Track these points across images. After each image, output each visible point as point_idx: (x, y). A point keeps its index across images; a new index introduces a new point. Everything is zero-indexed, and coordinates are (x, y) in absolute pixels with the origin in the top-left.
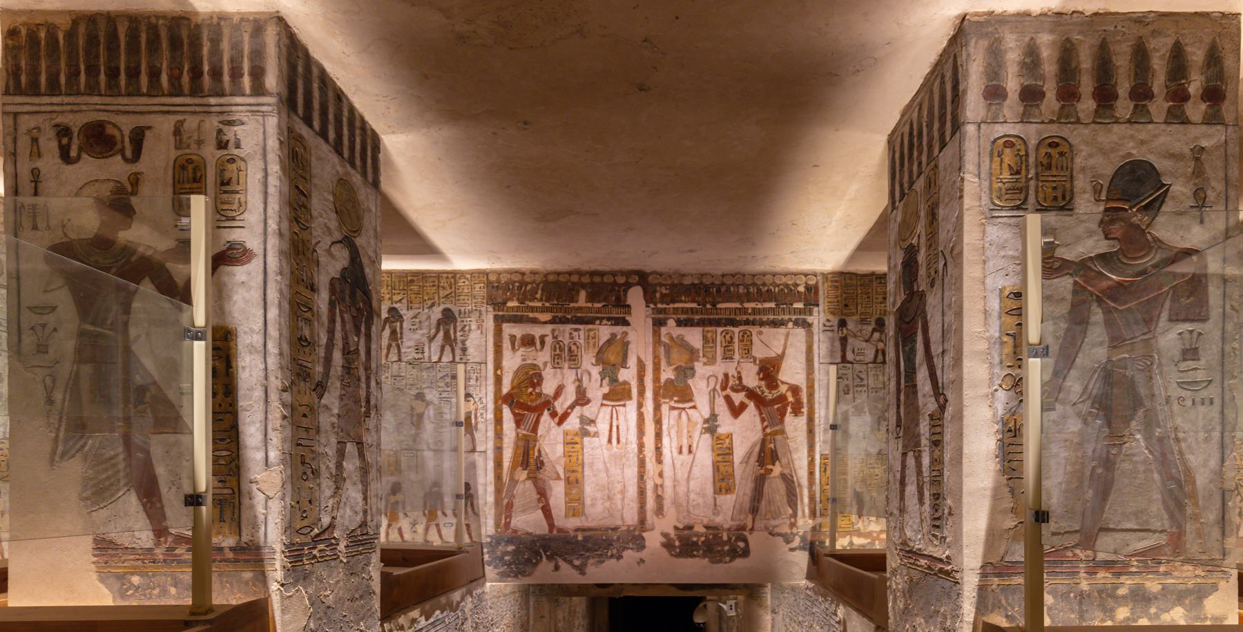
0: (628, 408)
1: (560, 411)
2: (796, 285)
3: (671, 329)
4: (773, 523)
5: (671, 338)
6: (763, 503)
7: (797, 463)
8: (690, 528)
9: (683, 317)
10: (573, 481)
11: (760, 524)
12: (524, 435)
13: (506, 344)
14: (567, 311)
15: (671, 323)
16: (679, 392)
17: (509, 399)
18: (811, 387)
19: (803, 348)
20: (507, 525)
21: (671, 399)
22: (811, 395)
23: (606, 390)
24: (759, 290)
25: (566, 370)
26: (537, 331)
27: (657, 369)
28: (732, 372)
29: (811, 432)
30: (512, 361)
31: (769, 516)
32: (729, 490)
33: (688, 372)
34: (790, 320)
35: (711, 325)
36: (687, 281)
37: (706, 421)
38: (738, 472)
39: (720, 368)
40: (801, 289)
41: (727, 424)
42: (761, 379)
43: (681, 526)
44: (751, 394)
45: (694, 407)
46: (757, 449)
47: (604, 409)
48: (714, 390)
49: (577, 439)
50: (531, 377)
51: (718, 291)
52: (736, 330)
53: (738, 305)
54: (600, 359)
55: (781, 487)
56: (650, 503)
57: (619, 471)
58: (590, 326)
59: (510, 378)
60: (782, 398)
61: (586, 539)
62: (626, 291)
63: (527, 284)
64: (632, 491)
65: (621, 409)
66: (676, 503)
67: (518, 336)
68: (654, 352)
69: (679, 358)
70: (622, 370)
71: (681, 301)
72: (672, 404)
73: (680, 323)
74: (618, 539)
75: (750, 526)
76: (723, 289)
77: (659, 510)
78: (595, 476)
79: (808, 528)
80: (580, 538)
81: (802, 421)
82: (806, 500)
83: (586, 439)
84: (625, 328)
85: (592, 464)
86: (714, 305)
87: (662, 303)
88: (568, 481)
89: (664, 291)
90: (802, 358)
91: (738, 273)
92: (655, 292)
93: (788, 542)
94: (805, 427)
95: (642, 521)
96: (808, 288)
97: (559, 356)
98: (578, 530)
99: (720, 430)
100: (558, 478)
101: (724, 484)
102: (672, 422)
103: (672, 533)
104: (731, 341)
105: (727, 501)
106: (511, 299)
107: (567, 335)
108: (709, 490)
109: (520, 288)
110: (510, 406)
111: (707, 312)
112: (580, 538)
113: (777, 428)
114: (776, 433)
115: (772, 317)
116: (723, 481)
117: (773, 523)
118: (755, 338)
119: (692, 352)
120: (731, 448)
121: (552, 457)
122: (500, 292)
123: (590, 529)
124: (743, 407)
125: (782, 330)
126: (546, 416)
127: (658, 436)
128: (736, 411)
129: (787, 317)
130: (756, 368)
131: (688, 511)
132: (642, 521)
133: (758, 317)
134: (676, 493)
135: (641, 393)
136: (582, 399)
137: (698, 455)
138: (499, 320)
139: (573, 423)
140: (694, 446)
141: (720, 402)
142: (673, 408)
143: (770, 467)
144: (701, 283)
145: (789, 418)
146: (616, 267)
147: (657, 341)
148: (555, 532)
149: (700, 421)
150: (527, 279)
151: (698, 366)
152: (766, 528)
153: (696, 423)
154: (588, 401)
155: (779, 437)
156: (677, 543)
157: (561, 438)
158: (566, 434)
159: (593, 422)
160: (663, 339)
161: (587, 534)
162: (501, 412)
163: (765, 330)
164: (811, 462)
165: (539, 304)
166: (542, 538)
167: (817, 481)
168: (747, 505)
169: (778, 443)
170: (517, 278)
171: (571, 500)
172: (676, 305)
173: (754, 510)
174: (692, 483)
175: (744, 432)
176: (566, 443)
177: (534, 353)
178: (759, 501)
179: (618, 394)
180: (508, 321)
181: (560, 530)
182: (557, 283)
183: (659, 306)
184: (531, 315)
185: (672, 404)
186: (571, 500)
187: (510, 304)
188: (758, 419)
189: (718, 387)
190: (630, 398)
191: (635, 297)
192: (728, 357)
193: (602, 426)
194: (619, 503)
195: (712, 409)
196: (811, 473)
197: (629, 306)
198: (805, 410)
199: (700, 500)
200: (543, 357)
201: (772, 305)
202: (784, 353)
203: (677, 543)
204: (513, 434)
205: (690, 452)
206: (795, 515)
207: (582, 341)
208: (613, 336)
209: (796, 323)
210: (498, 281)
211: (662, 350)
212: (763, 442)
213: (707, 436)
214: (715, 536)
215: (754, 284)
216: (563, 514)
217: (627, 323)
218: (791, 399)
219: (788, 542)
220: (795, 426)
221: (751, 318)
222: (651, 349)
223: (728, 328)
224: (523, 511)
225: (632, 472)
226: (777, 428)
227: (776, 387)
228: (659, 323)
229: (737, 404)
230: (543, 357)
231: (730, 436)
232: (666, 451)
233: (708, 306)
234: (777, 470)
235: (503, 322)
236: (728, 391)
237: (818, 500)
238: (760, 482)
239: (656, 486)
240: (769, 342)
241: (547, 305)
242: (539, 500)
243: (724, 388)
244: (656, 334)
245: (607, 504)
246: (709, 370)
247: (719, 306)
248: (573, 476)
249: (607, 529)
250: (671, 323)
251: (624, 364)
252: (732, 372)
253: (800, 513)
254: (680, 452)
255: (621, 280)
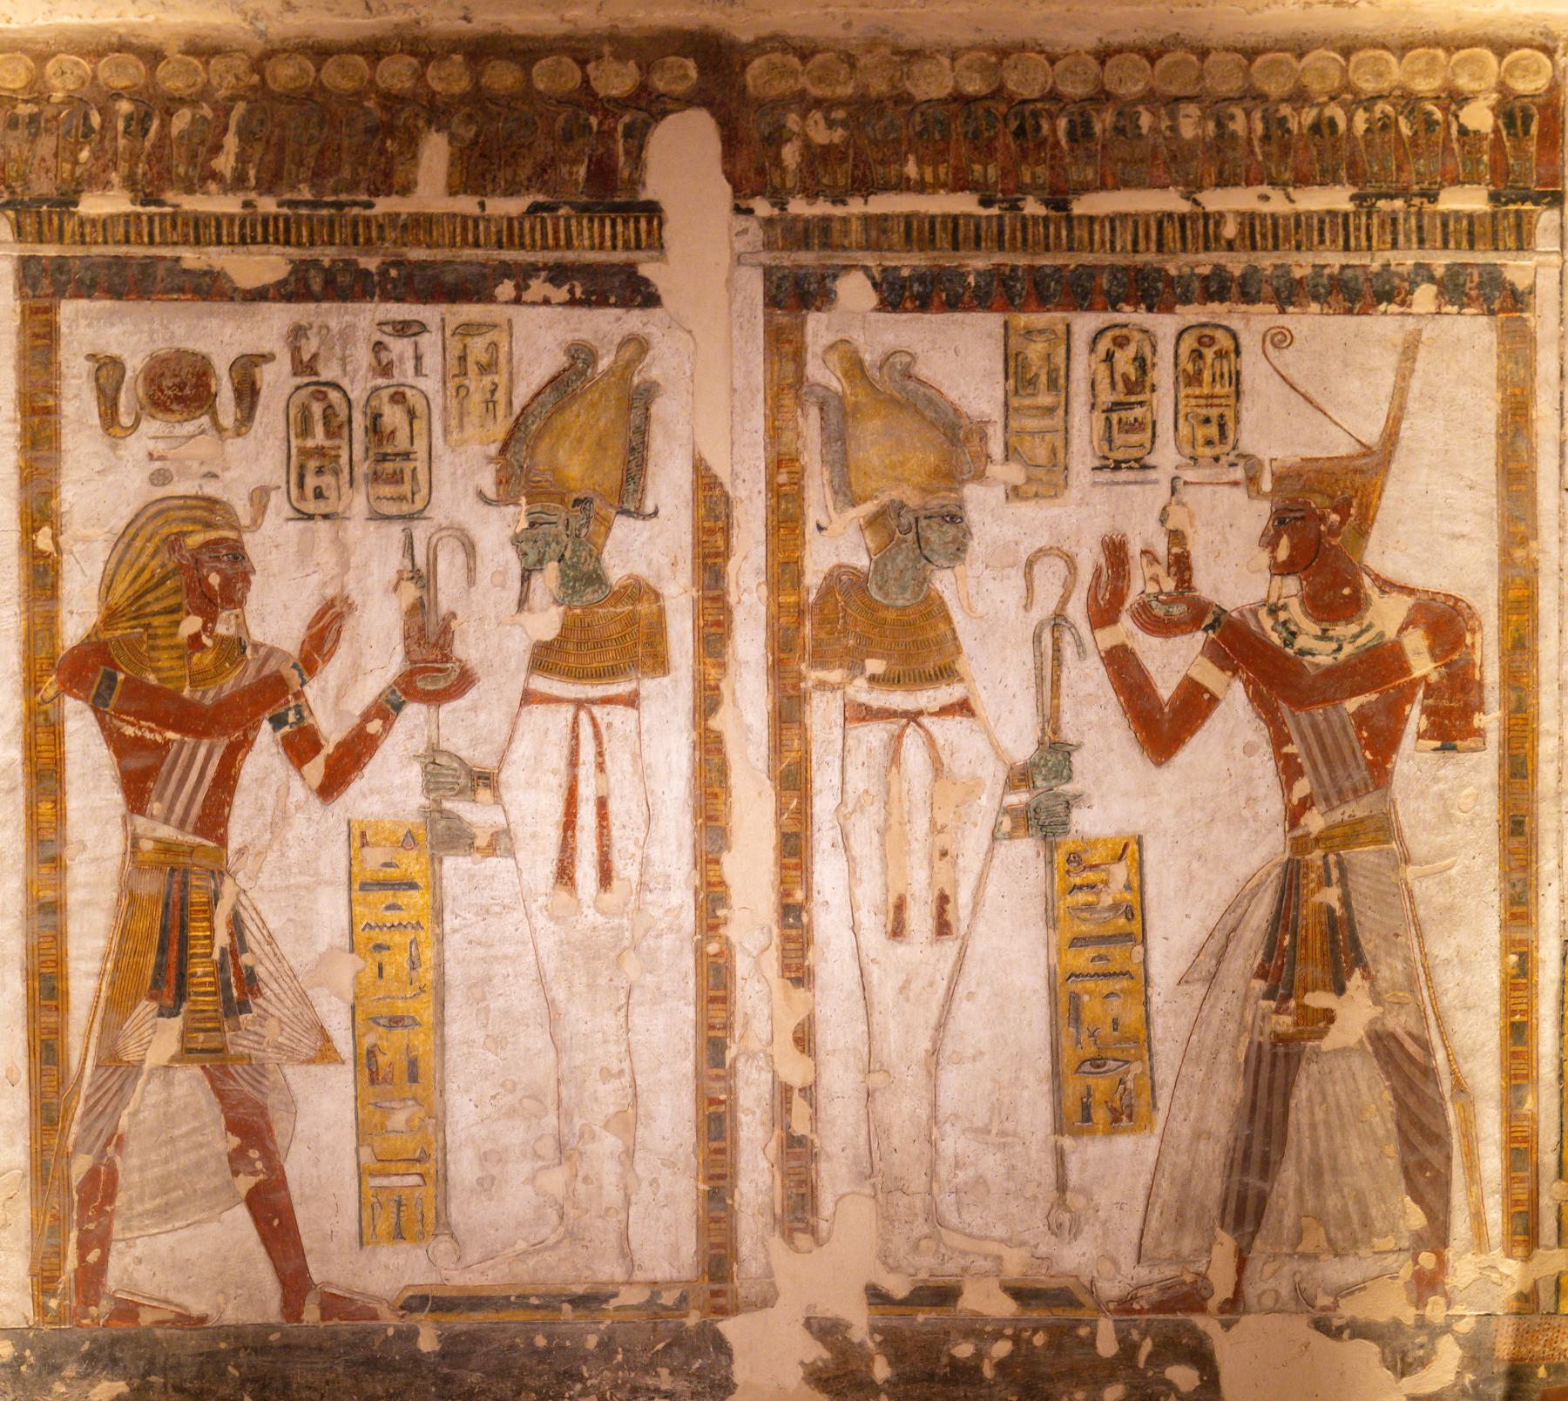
0: (651, 711)
1: (332, 729)
2: (1456, 99)
3: (852, 318)
4: (1336, 1272)
5: (855, 367)
6: (1288, 1175)
7: (1448, 980)
8: (943, 1295)
9: (910, 262)
10: (396, 1072)
11: (1270, 1278)
12: (166, 847)
13: (77, 401)
14: (362, 234)
15: (855, 291)
16: (890, 633)
17: (94, 671)
18: (1520, 605)
19: (1488, 410)
20: (91, 1278)
21: (854, 665)
22: (1520, 646)
23: (546, 623)
24: (1276, 127)
25: (357, 529)
26: (220, 337)
27: (786, 522)
28: (1144, 533)
29: (1517, 828)
30: (105, 487)
31: (1314, 1239)
32: (1124, 1115)
33: (935, 535)
34: (1423, 272)
35: (1042, 299)
36: (932, 84)
37: (1020, 777)
38: (1169, 1030)
39: (1085, 513)
40: (1479, 117)
41: (1117, 790)
42: (1281, 570)
43: (898, 1287)
44: (1236, 644)
45: (963, 708)
46: (1261, 912)
47: (537, 715)
48: (1058, 621)
49: (412, 864)
50: (192, 566)
51: (1080, 132)
52: (1165, 325)
53: (1171, 201)
54: (517, 471)
55: (1373, 1095)
56: (757, 1177)
57: (610, 1022)
58: (470, 312)
59: (96, 570)
60: (1381, 664)
61: (455, 1349)
62: (637, 137)
63: (171, 104)
64: (672, 1118)
65: (618, 716)
66: (873, 1173)
67: (135, 364)
68: (774, 433)
69: (892, 459)
70: (622, 528)
71: (902, 185)
72: (861, 692)
73: (895, 295)
74: (607, 1346)
75: (1222, 1287)
76: (1103, 122)
77: (799, 1210)
78: (497, 1042)
79: (1500, 1300)
80: (427, 1342)
81: (1475, 774)
82: (1492, 1163)
83: (454, 866)
84: (633, 320)
85: (480, 987)
86: (1058, 201)
87: (812, 196)
88: (370, 1067)
89: (821, 135)
90: (1482, 460)
91: (1177, 42)
92: (776, 139)
93: (1403, 1365)
94: (1489, 808)
95: (718, 1261)
96: (1512, 114)
97: (325, 459)
98: (416, 1303)
99: (1088, 822)
100: (325, 1053)
101: (1101, 1085)
102: (859, 780)
103: (860, 1322)
104: (1139, 383)
105: (1119, 1165)
106: (95, 181)
107: (362, 356)
108: (1034, 1110)
109: (138, 124)
110: (98, 706)
111: (1025, 235)
112: (427, 1342)
113: (1357, 809)
114: (1351, 834)
115: (1334, 259)
116: (1097, 1075)
117: (1336, 1272)
118: (1253, 367)
119: (955, 435)
120: (1134, 911)
121: (297, 955)
122: (46, 145)
123: (474, 1302)
124: (1194, 705)
125: (1385, 325)
126: (265, 754)
127: (794, 848)
128: (1163, 726)
129: (1406, 259)
130: (1256, 515)
131: (934, 1217)
132: (718, 1261)
133: (1266, 261)
134: (875, 1129)
135: (714, 635)
136: (433, 671)
137: (978, 947)
138: (43, 287)
139: (391, 786)
140: (964, 897)
141: (1087, 679)
142: (866, 714)
143: (1319, 999)
144: (998, 92)
145: (1413, 759)
146: (585, 17)
147: (787, 382)
148: (311, 1314)
149: (992, 775)
150: (172, 80)
151: (983, 504)
152: (1302, 1298)
153: (973, 788)
154: (465, 681)
155: (1363, 856)
156: (881, 1370)
157: (334, 860)
158: (359, 838)
159: (484, 780)
160: (816, 371)
161: (462, 1322)
162: (56, 732)
163: (1306, 322)
164: (1519, 979)
165: (229, 205)
166: (251, 1341)
167: (1547, 1071)
168: (1211, 1187)
169: (1361, 885)
170: (123, 74)
171: (386, 1163)
172: (881, 204)
173: (1245, 1212)
174: (952, 1081)
175: (1201, 827)
176: (362, 885)
177: (204, 446)
178: (1267, 1169)
179: (602, 643)
180: (86, 289)
181: (333, 1305)
182: (310, 99)
183: (798, 207)
184: (191, 258)
185: (861, 692)
186: (386, 1163)
187: (93, 205)
188: (1265, 767)
189: (1077, 611)
190: (658, 663)
191: (683, 162)
192: (1123, 461)
193: (531, 802)
194: (609, 1173)
195: (1050, 719)
196: (1518, 1032)
197: (652, 210)
198: (1490, 720)
199: (991, 1164)
200: (246, 464)
201: (1338, 198)
202: (1391, 437)
203: (881, 1370)
204: (115, 844)
205: (943, 927)
206: (1437, 1235)
207: (431, 384)
208: (581, 356)
209: (1453, 289)
210: (37, 91)
211: (810, 426)
212: (1292, 880)
213: (1026, 848)
214: (1061, 1335)
215: (1252, 96)
216: (348, 1224)
217: (643, 295)
218: (1423, 665)
219: (1403, 1365)
220: (1440, 796)
221: (1236, 264)
222: (757, 420)
223: (1131, 316)
224: (165, 1213)
225: (668, 1026)
226: (1357, 809)
227: (1354, 606)
228: (795, 295)
229: (1166, 690)
230: (246, 464)
231: (1130, 849)
232: (828, 924)
233: (1032, 207)
234: (1354, 1014)
235: (60, 293)
236: (1126, 630)
237: (1548, 1159)
238: (1272, 1072)
239: (784, 1093)
240: (1319, 383)
241: (268, 205)
242: (237, 1159)
243: (1103, 616)
244: (784, 344)
245: (555, 1180)
246: (1032, 524)
247: (1080, 207)
248: (392, 1046)
249: (551, 1302)
250: (855, 291)
251: (628, 490)
252: (1144, 533)
253: (1460, 1226)
254: (897, 930)
255: (616, 80)
